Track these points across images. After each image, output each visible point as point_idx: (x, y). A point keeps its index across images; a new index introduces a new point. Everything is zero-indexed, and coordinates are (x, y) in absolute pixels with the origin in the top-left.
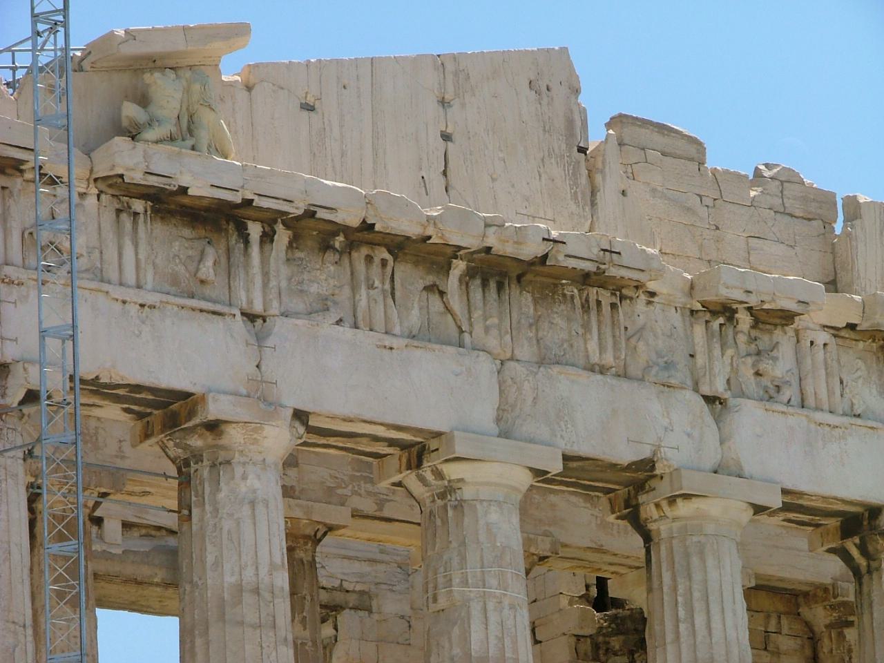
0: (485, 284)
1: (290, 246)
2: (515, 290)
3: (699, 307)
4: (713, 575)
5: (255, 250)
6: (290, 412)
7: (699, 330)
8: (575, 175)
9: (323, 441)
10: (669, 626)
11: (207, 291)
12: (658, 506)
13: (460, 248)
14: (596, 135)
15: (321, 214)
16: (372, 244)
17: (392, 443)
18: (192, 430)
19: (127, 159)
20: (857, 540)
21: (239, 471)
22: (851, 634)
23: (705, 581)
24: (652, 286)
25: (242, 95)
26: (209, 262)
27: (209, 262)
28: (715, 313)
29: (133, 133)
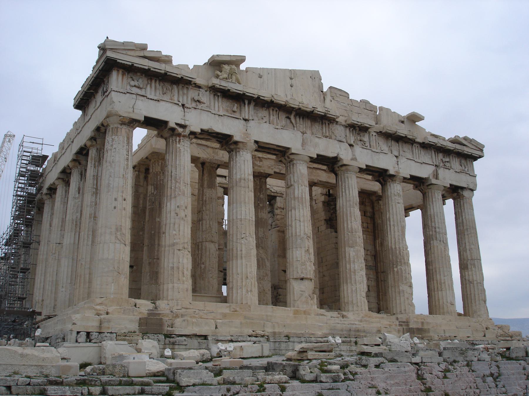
0: (300, 118)
2: (307, 120)
5: (246, 106)
7: (348, 129)
8: (320, 96)
9: (263, 150)
10: (341, 193)
11: (235, 114)
12: (338, 167)
13: (293, 108)
14: (325, 90)
15: (261, 98)
16: (274, 107)
17: (278, 151)
18: (231, 144)
19: (216, 82)
21: (241, 153)
22: (381, 202)
24: (337, 120)
25: (245, 73)
26: (235, 107)
27: (235, 107)
29: (217, 77)
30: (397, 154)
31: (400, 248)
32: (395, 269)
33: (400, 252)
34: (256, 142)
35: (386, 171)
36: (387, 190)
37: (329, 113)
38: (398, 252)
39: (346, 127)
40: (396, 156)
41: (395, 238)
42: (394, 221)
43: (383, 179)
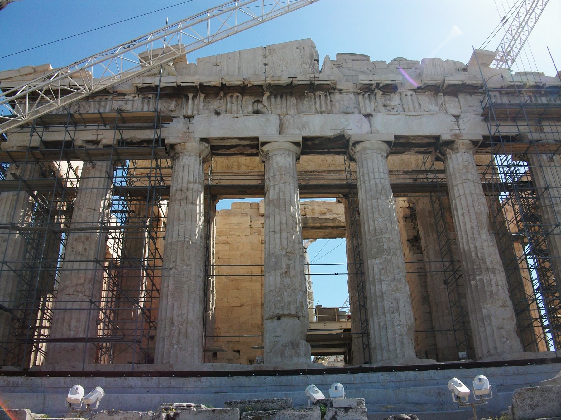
0: (276, 97)
1: (205, 98)
2: (289, 98)
3: (359, 91)
4: (370, 164)
5: (190, 101)
6: (198, 139)
7: (360, 97)
13: (261, 86)
15: (205, 84)
20: (438, 151)
23: (368, 167)
28: (366, 92)
30: (456, 113)
31: (476, 247)
32: (473, 283)
33: (476, 254)
34: (203, 140)
35: (438, 138)
36: (449, 166)
37: (316, 79)
38: (473, 254)
39: (359, 94)
40: (454, 116)
41: (466, 232)
42: (462, 208)
43: (440, 153)
